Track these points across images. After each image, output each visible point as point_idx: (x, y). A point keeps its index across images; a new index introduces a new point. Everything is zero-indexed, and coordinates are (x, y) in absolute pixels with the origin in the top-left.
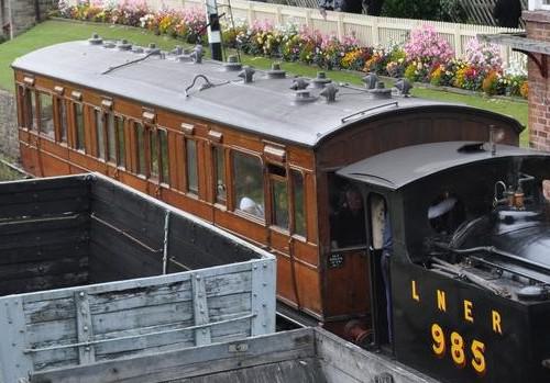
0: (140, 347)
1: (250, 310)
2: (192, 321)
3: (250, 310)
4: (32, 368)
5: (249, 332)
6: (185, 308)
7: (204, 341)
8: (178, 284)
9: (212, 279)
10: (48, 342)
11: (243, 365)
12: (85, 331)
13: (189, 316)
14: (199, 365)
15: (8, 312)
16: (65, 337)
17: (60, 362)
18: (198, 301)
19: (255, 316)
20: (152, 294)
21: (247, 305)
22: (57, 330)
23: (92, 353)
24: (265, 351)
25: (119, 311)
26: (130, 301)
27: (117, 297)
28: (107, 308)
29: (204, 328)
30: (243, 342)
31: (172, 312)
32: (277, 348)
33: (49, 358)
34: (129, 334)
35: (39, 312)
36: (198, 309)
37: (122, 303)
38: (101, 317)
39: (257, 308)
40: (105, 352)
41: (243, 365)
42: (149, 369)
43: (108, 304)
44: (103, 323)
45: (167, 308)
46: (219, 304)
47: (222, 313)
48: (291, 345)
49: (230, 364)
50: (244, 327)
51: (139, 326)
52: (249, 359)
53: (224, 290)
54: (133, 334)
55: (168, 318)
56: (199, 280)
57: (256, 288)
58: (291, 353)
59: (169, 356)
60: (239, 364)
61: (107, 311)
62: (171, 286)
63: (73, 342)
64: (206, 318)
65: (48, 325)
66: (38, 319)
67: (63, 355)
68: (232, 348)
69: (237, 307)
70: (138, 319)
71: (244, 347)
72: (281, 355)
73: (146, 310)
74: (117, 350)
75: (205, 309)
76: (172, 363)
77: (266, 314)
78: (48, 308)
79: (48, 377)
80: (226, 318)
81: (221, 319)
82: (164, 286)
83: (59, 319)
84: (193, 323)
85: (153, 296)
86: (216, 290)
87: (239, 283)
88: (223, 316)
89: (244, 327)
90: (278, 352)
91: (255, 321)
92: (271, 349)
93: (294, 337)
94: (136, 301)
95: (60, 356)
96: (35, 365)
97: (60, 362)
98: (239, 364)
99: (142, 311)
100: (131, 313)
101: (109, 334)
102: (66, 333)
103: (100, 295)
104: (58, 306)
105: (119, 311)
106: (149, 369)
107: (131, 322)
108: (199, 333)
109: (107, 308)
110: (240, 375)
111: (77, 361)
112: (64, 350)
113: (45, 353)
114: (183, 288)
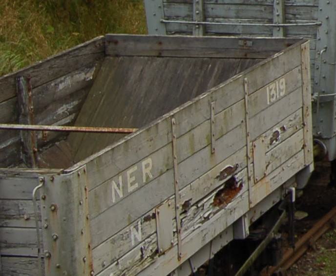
0: (238, 32)
1: (317, 20)
10: (177, 17)
11: (248, 56)
12: (198, 14)
14: (218, 50)
18: (275, 6)
21: (315, 16)
23: (201, 29)
29: (279, 26)
31: (262, 11)
33: (176, 28)
34: (230, 21)
38: (212, 6)
39: (321, 19)
40: (214, 31)
41: (248, 56)
42: (184, 46)
44: (214, 10)
45: (258, 8)
46: (295, 11)
47: (297, 18)
49: (241, 55)
51: (237, 17)
52: (254, 52)
54: (233, 22)
55: (258, 14)
60: (246, 55)
64: (281, 19)
65: (177, 6)
67: (186, 27)
68: (241, 43)
69: (308, 16)
70: (238, 11)
73: (244, 7)
74: (221, 31)
75: (280, 12)
80: (300, 22)
88: (297, 21)
91: (320, 28)
95: (184, 28)
96: (167, 32)
98: (246, 55)
99: (240, 7)
100: (233, 7)
101: (217, 19)
106: (184, 46)
107: (233, 14)
108: (275, 31)
112: (187, 24)
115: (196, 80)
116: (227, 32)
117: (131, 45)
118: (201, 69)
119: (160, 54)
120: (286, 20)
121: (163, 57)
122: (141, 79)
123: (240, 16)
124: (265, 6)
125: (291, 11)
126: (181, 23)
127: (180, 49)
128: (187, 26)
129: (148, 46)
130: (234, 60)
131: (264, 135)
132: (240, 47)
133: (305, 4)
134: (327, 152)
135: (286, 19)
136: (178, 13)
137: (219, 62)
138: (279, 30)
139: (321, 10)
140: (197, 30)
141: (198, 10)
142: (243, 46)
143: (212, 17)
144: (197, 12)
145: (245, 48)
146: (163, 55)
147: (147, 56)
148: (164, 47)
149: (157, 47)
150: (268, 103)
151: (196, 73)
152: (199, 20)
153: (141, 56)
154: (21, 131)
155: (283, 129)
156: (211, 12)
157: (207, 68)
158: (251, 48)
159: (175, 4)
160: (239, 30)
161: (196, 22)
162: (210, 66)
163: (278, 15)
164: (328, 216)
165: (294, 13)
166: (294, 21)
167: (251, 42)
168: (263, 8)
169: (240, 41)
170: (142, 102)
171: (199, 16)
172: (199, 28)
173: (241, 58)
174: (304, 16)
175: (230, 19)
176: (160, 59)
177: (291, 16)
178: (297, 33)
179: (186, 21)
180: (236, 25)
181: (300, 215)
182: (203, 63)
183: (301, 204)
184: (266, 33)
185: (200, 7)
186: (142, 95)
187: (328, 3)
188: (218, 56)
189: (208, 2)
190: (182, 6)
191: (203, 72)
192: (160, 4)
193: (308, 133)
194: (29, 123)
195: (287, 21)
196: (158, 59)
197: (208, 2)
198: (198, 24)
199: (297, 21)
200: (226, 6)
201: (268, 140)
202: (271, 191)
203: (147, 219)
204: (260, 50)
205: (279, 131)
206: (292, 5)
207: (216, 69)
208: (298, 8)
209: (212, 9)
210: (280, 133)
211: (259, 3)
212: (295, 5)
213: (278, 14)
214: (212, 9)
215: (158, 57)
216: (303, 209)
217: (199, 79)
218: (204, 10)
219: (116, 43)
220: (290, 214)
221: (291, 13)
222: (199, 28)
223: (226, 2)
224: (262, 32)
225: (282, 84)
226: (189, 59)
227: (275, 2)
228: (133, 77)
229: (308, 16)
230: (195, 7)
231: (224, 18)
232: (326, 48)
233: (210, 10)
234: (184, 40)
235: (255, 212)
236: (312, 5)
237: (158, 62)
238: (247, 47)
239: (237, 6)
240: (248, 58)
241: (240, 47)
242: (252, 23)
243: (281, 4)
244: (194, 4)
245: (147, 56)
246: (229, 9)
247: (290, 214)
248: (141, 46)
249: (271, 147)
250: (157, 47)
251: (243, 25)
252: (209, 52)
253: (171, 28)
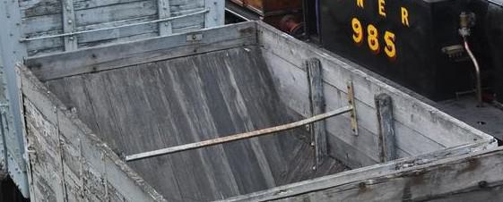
1: (204, 7)
2: (157, 16)
3: (204, 7)
4: (27, 54)
5: (203, 25)
6: (151, 5)
7: (166, 32)
10: (39, 33)
12: (70, 24)
13: (154, 12)
14: (162, 52)
15: (7, 7)
16: (53, 29)
17: (49, 49)
19: (208, 12)
22: (46, 23)
23: (75, 41)
24: (216, 40)
25: (97, 7)
28: (87, 5)
30: (198, 33)
31: (141, 8)
32: (227, 37)
33: (40, 45)
34: (105, 26)
35: (32, 8)
36: (161, 6)
38: (82, 12)
42: (122, 55)
44: (84, 17)
47: (182, 9)
48: (237, 35)
49: (187, 51)
50: (199, 21)
51: (113, 20)
52: (203, 46)
54: (108, 26)
55: (137, 13)
58: (238, 42)
59: (138, 44)
60: (195, 51)
61: (87, 8)
63: (59, 33)
64: (168, 14)
65: (39, 19)
67: (51, 43)
70: (112, 14)
71: (199, 37)
72: (229, 43)
73: (120, 6)
74: (95, 39)
75: (167, 6)
76: (140, 49)
77: (217, 10)
79: (39, 61)
80: (185, 13)
81: (180, 14)
83: (48, 14)
84: (158, 18)
88: (182, 12)
89: (199, 21)
90: (227, 41)
91: (208, 16)
92: (220, 38)
93: (239, 29)
95: (49, 44)
96: (28, 52)
97: (49, 49)
100: (107, 9)
101: (88, 26)
102: (54, 25)
105: (97, 7)
106: (122, 55)
107: (106, 17)
108: (162, 25)
110: (195, 60)
111: (63, 48)
112: (52, 39)
113: (37, 42)
115: (157, 88)
117: (59, 65)
122: (90, 100)
129: (78, 63)
136: (40, 28)
148: (99, 60)
149: (90, 61)
151: (151, 81)
154: (287, 133)
160: (115, 34)
167: (201, 35)
170: (112, 124)
171: (70, 26)
176: (97, 76)
182: (150, 69)
185: (72, 15)
188: (165, 57)
190: (46, 19)
191: (158, 78)
194: (140, 149)
196: (93, 75)
198: (72, 36)
200: (98, 9)
204: (211, 41)
207: (170, 72)
215: (92, 73)
217: (159, 85)
219: (39, 66)
223: (99, 5)
231: (97, 23)
237: (97, 79)
241: (187, 43)
246: (102, 12)
248: (71, 64)
250: (90, 61)
253: (32, 47)
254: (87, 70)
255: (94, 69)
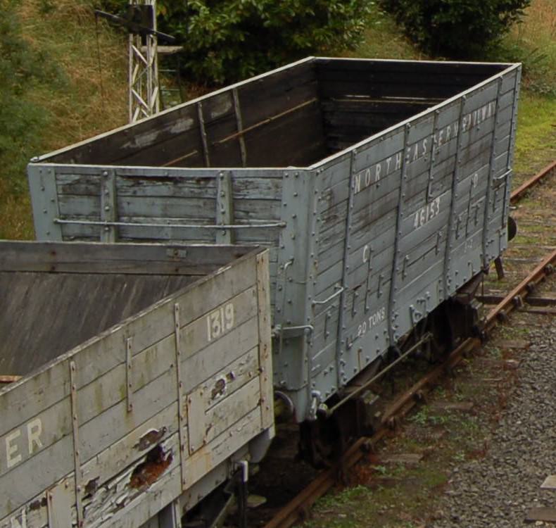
0: (165, 237)
1: (279, 219)
8: (207, 179)
9: (241, 180)
10: (78, 216)
12: (108, 210)
14: (137, 264)
15: (41, 178)
18: (220, 200)
19: (284, 226)
20: (180, 185)
21: (277, 214)
22: (86, 205)
23: (113, 232)
25: (146, 196)
26: (156, 188)
27: (145, 182)
28: (135, 192)
29: (224, 229)
31: (200, 207)
33: (77, 231)
34: (154, 221)
35: (70, 184)
37: (150, 189)
38: (128, 199)
39: (286, 219)
40: (130, 236)
41: (180, 272)
42: (87, 258)
43: (136, 188)
44: (131, 206)
45: (194, 202)
46: (248, 207)
47: (251, 217)
49: (170, 270)
52: (188, 267)
53: (253, 194)
54: (159, 222)
55: (195, 212)
56: (222, 178)
57: (287, 197)
60: (177, 270)
61: (134, 195)
62: (199, 180)
65: (78, 199)
66: (69, 191)
68: (170, 252)
69: (267, 214)
70: (165, 207)
73: (175, 200)
74: (142, 235)
75: (226, 208)
78: (78, 182)
80: (256, 223)
82: (192, 179)
83: (89, 194)
85: (180, 188)
86: (246, 191)
87: (269, 188)
88: (251, 220)
91: (284, 232)
94: (164, 189)
95: (88, 231)
96: (63, 236)
98: (177, 270)
99: (169, 201)
100: (159, 201)
101: (135, 219)
103: (129, 177)
104: (88, 181)
105: (146, 196)
106: (87, 258)
107: (158, 211)
108: (219, 235)
109: (135, 192)
112: (92, 226)
114: (211, 184)
116: (150, 237)
118: (113, 290)
119: (53, 268)
120: (234, 219)
121: (57, 273)
122: (25, 304)
123: (169, 213)
124: (206, 200)
125: (242, 207)
126: (83, 224)
127: (82, 261)
128: (92, 228)
129: (36, 257)
130: (160, 277)
131: (203, 385)
132: (168, 259)
133: (262, 197)
134: (294, 410)
135: (235, 218)
137: (138, 280)
138: (225, 234)
139: (285, 205)
140: (107, 234)
141: (107, 205)
142: (173, 257)
143: (128, 216)
144: (107, 208)
145: (175, 259)
146: (57, 270)
147: (34, 272)
148: (59, 258)
149: (48, 258)
150: (209, 339)
151: (106, 296)
152: (109, 219)
153: (25, 271)
155: (231, 376)
156: (127, 208)
157: (122, 288)
158: (184, 261)
159: (76, 197)
160: (167, 234)
161: (105, 223)
162: (125, 285)
163: (223, 213)
164: (296, 502)
165: (246, 210)
166: (245, 221)
167: (185, 252)
168: (201, 203)
169: (168, 250)
170: (27, 338)
171: (109, 214)
172: (109, 231)
173: (170, 275)
174: (260, 215)
175: (154, 219)
176: (53, 276)
177: (242, 214)
178: (251, 238)
179: (91, 221)
180: (163, 227)
181: (256, 501)
182: (115, 281)
183: (256, 485)
184: (206, 238)
185: (111, 201)
186: (27, 328)
187: (296, 196)
189: (123, 194)
190: (85, 199)
191: (115, 294)
192: (54, 197)
193: (267, 382)
195: (237, 220)
196: (51, 275)
197: (123, 194)
198: (108, 226)
199: (251, 220)
200: (148, 199)
201: (208, 393)
202: (213, 466)
203: (35, 506)
205: (225, 379)
206: (243, 199)
207: (134, 290)
208: (253, 202)
209: (129, 203)
210: (226, 382)
211: (196, 196)
212: (247, 197)
213: (222, 210)
214: (129, 203)
215: (50, 272)
216: (258, 491)
217: (110, 304)
218: (117, 205)
220: (240, 499)
221: (242, 209)
222: (109, 231)
223: (149, 194)
224: (200, 238)
225: (228, 312)
226: (95, 275)
227: (219, 195)
228: (14, 302)
229: (267, 214)
230: (103, 202)
231: (145, 216)
232: (293, 260)
233: (125, 205)
234: (87, 249)
235: (190, 496)
236: (272, 198)
238: (178, 258)
239: (166, 199)
240: (180, 275)
241: (168, 259)
242: (185, 224)
243: (227, 197)
244: (102, 197)
245: (34, 272)
246: (153, 204)
247: (240, 499)
248: (25, 257)
249: (213, 403)
250: (48, 258)
251: (172, 227)
252: (126, 266)
253: (69, 231)
254: (45, 268)
255: (53, 268)
